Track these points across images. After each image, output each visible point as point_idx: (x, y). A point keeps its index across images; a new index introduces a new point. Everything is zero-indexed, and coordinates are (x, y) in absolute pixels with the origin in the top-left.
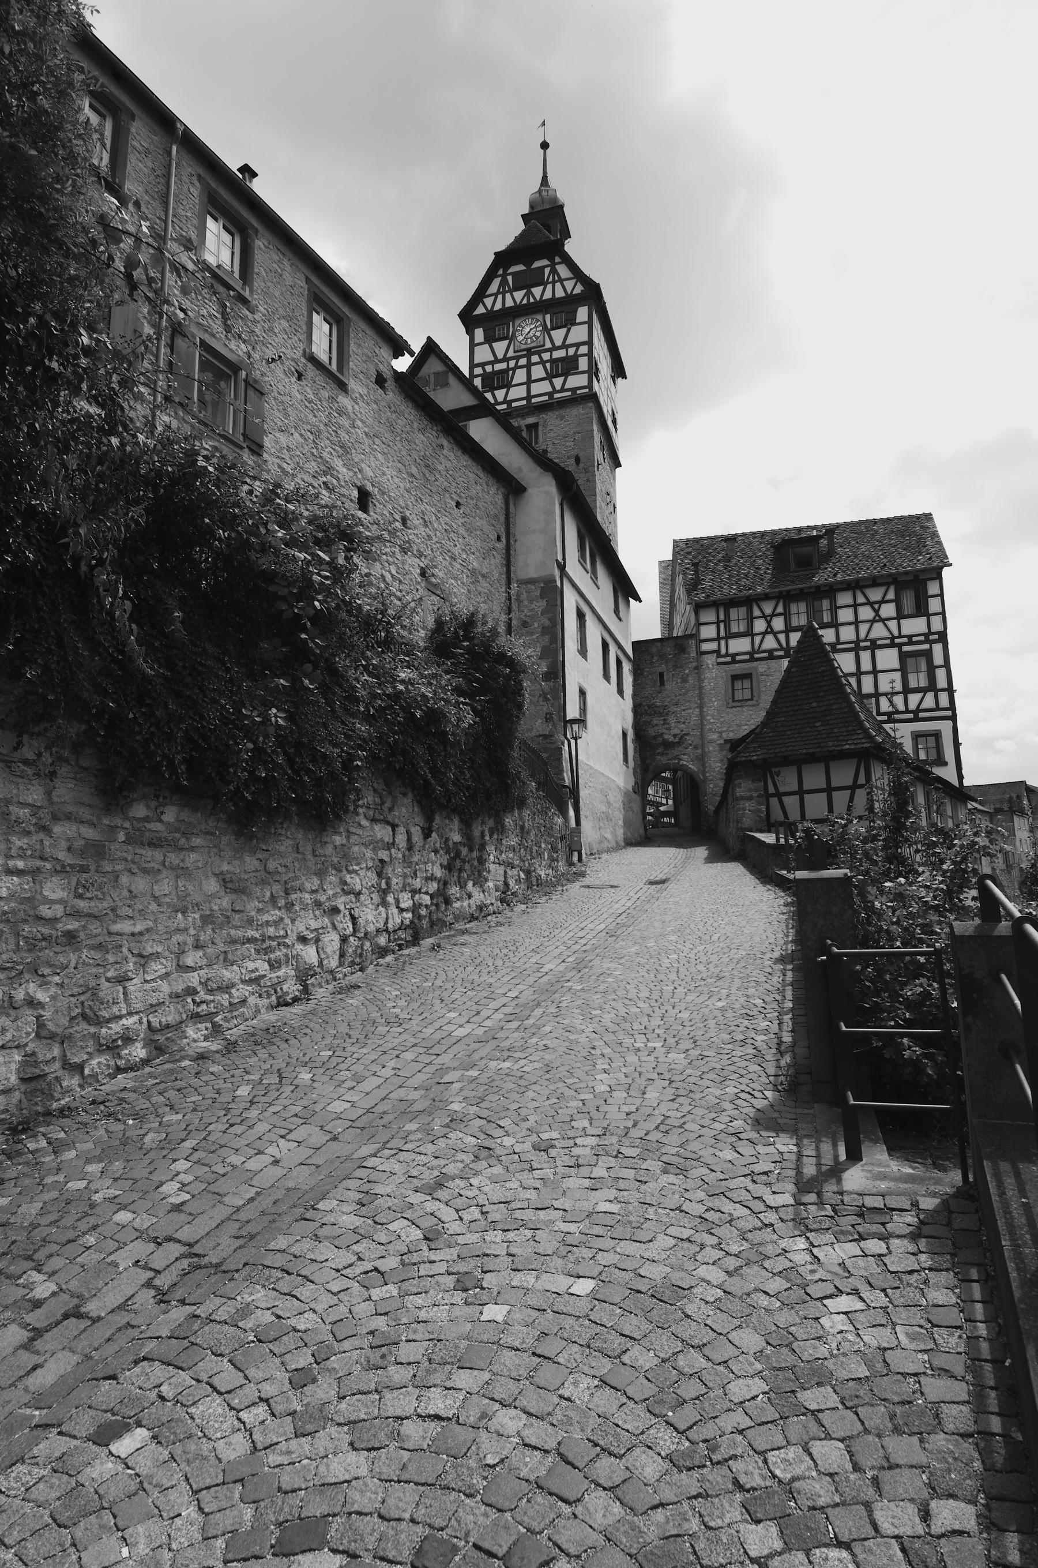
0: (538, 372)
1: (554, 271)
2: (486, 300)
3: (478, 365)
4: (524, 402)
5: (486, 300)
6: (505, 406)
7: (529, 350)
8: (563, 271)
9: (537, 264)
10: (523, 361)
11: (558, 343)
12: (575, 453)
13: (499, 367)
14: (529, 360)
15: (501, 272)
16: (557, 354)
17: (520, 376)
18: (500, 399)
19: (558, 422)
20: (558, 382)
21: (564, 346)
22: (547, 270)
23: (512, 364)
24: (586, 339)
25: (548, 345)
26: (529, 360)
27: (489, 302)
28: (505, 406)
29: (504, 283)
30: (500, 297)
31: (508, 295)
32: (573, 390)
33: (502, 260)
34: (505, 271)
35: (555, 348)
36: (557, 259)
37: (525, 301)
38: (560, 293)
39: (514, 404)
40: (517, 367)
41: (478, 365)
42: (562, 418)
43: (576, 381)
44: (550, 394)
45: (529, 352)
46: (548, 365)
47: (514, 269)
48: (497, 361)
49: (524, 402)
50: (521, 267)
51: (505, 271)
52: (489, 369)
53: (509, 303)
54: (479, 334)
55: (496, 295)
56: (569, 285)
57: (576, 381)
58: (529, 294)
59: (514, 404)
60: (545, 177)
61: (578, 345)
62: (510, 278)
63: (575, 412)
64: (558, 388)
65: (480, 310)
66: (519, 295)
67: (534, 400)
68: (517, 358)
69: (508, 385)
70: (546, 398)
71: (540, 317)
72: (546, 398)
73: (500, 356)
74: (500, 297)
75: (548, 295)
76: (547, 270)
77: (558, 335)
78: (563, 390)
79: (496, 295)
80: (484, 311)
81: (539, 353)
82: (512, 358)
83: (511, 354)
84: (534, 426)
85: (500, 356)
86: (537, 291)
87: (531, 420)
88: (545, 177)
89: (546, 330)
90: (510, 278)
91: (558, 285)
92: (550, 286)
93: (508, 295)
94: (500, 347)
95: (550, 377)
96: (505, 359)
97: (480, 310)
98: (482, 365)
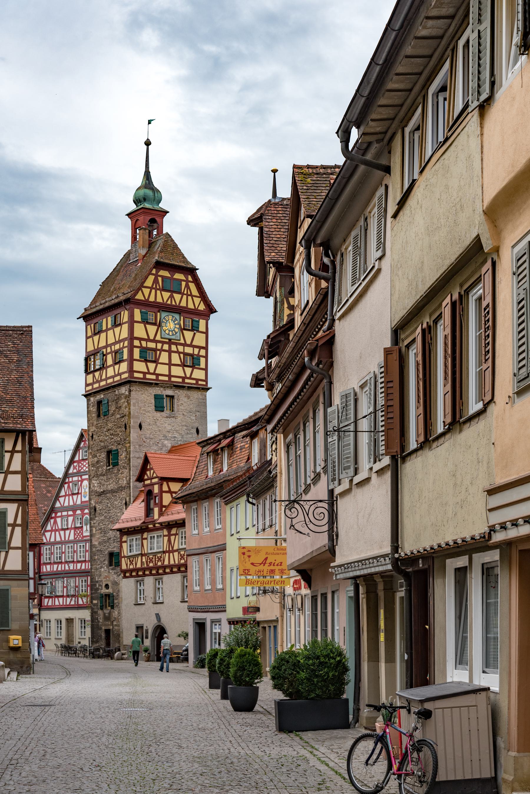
0: (175, 358)
1: (187, 286)
4: (166, 379)
6: (154, 377)
7: (170, 340)
9: (178, 276)
10: (166, 347)
11: (188, 342)
12: (196, 425)
13: (152, 345)
14: (170, 347)
15: (154, 271)
16: (189, 350)
17: (164, 357)
18: (152, 371)
19: (186, 400)
20: (188, 370)
21: (191, 345)
22: (184, 284)
23: (159, 346)
24: (204, 345)
25: (182, 341)
26: (170, 347)
28: (154, 377)
29: (156, 281)
30: (153, 291)
31: (158, 292)
32: (197, 380)
34: (157, 272)
35: (185, 345)
37: (169, 302)
39: (161, 378)
40: (162, 350)
42: (189, 397)
43: (198, 374)
44: (184, 378)
45: (170, 342)
46: (182, 355)
47: (163, 273)
48: (148, 340)
50: (166, 274)
51: (157, 272)
52: (144, 344)
55: (151, 288)
56: (197, 300)
57: (198, 374)
58: (171, 297)
59: (161, 378)
60: (147, 175)
61: (200, 348)
62: (160, 279)
63: (195, 395)
64: (188, 376)
66: (166, 295)
67: (173, 379)
68: (163, 343)
70: (180, 380)
71: (177, 316)
72: (180, 380)
75: (183, 304)
76: (184, 284)
77: (188, 335)
78: (190, 378)
81: (176, 344)
83: (158, 338)
84: (172, 397)
85: (152, 337)
86: (177, 297)
87: (170, 392)
88: (147, 175)
89: (182, 330)
90: (160, 279)
91: (190, 298)
93: (158, 292)
94: (152, 329)
95: (183, 365)
96: (154, 341)
98: (140, 339)
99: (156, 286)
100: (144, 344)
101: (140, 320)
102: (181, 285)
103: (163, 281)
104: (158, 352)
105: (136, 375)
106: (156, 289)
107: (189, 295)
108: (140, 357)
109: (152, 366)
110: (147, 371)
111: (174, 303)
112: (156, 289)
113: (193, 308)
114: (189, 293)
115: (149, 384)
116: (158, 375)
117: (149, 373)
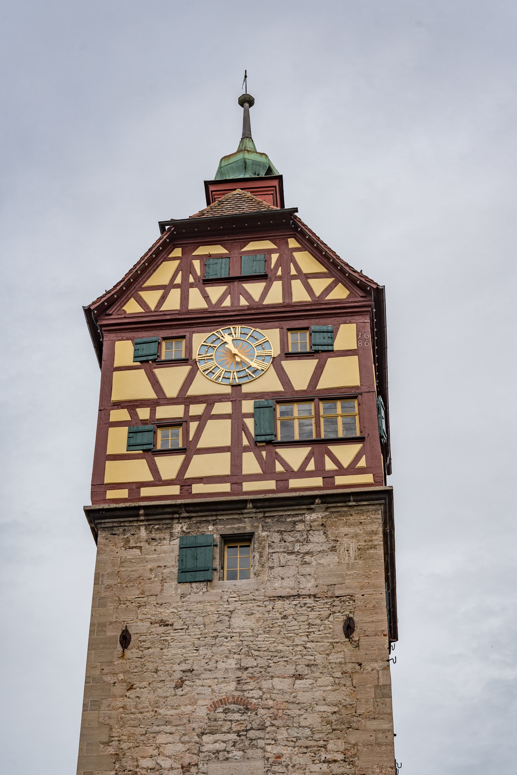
1: (286, 260)
2: (143, 294)
3: (119, 405)
4: (226, 487)
5: (143, 294)
8: (306, 262)
15: (177, 252)
22: (275, 257)
23: (197, 409)
27: (151, 299)
28: (175, 490)
29: (186, 268)
31: (194, 294)
33: (179, 235)
36: (293, 243)
37: (227, 303)
38: (299, 294)
41: (119, 405)
47: (202, 251)
49: (226, 487)
52: (144, 413)
53: (196, 301)
54: (124, 351)
55: (166, 289)
62: (197, 264)
65: (132, 307)
67: (247, 486)
69: (188, 450)
73: (171, 391)
74: (175, 295)
76: (275, 257)
79: (166, 289)
80: (139, 309)
82: (197, 400)
86: (255, 289)
90: (197, 264)
91: (297, 285)
92: (277, 287)
97: (132, 307)
98: (132, 405)
99: (185, 278)
100: (144, 413)
101: (130, 362)
102: (267, 261)
103: (204, 266)
104: (193, 426)
105: (111, 494)
106: (185, 288)
107: (295, 277)
108: (130, 446)
109: (169, 466)
110: (149, 477)
111: (243, 302)
112: (185, 288)
113: (307, 298)
114: (293, 272)
115: (160, 514)
116: (185, 483)
117: (158, 482)
